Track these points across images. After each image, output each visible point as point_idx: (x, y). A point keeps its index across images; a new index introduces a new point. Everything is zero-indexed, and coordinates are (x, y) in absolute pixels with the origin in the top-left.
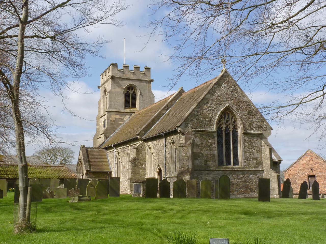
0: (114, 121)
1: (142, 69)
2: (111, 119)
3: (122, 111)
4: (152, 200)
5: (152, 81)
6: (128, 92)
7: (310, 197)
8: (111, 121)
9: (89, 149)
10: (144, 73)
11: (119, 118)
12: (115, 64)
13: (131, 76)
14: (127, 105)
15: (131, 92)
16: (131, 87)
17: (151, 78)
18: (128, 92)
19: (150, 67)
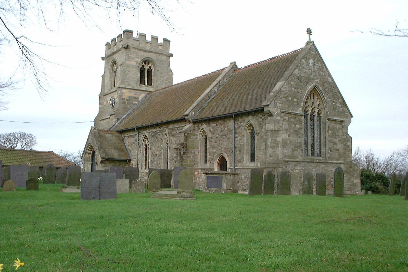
0: (127, 100)
1: (160, 41)
2: (124, 97)
3: (136, 88)
4: (168, 189)
5: (171, 55)
6: (143, 66)
7: (330, 191)
8: (124, 99)
9: (102, 132)
10: (163, 46)
11: (134, 97)
12: (130, 31)
13: (148, 47)
14: (142, 82)
15: (147, 67)
16: (146, 61)
17: (170, 53)
18: (143, 66)
19: (168, 39)
